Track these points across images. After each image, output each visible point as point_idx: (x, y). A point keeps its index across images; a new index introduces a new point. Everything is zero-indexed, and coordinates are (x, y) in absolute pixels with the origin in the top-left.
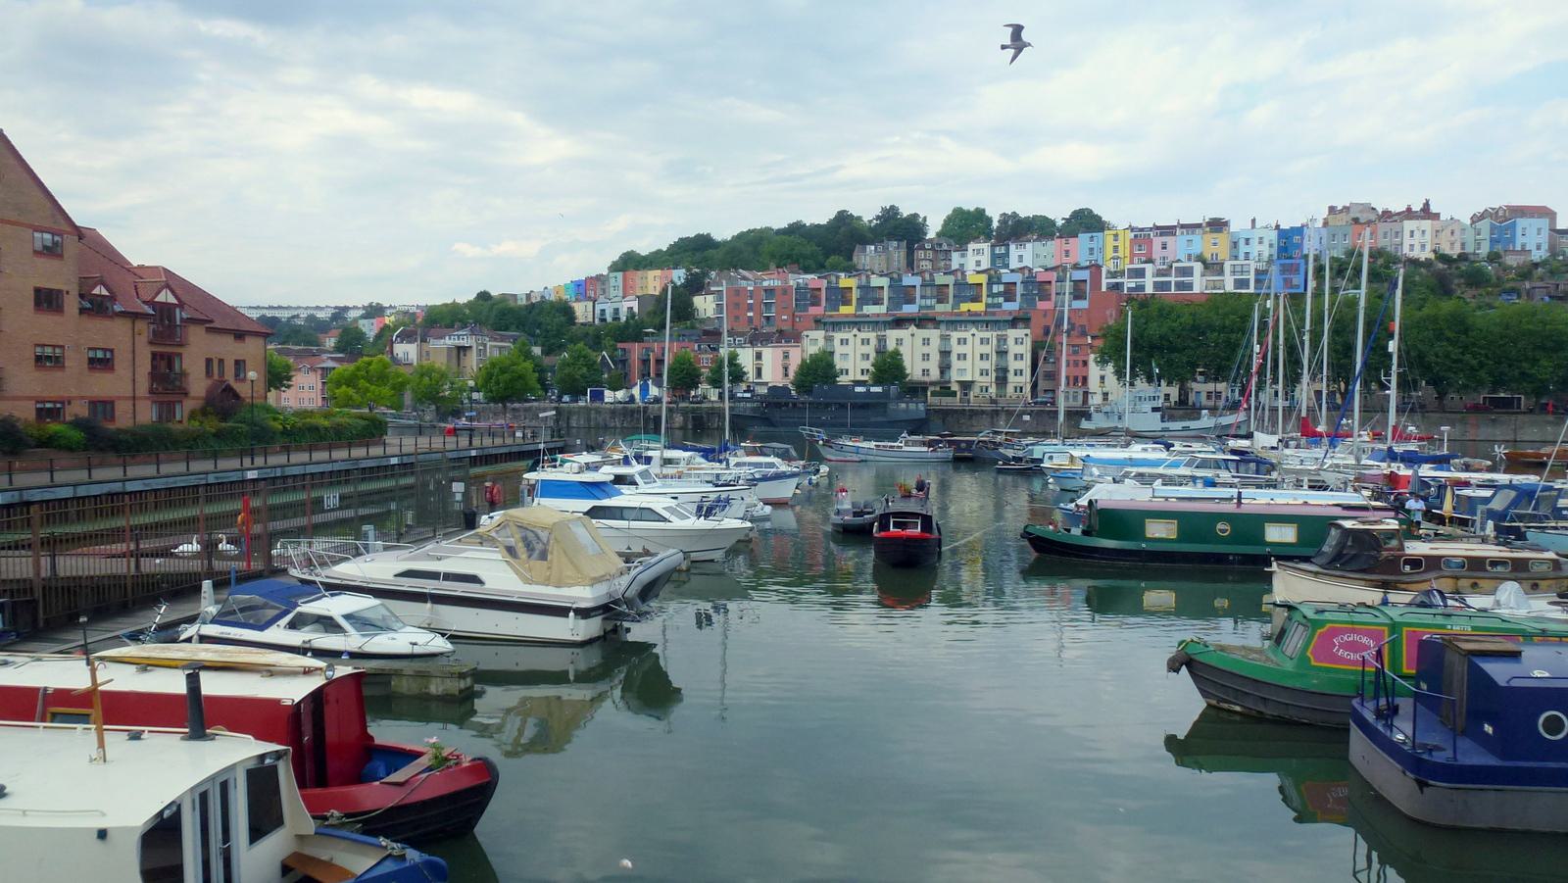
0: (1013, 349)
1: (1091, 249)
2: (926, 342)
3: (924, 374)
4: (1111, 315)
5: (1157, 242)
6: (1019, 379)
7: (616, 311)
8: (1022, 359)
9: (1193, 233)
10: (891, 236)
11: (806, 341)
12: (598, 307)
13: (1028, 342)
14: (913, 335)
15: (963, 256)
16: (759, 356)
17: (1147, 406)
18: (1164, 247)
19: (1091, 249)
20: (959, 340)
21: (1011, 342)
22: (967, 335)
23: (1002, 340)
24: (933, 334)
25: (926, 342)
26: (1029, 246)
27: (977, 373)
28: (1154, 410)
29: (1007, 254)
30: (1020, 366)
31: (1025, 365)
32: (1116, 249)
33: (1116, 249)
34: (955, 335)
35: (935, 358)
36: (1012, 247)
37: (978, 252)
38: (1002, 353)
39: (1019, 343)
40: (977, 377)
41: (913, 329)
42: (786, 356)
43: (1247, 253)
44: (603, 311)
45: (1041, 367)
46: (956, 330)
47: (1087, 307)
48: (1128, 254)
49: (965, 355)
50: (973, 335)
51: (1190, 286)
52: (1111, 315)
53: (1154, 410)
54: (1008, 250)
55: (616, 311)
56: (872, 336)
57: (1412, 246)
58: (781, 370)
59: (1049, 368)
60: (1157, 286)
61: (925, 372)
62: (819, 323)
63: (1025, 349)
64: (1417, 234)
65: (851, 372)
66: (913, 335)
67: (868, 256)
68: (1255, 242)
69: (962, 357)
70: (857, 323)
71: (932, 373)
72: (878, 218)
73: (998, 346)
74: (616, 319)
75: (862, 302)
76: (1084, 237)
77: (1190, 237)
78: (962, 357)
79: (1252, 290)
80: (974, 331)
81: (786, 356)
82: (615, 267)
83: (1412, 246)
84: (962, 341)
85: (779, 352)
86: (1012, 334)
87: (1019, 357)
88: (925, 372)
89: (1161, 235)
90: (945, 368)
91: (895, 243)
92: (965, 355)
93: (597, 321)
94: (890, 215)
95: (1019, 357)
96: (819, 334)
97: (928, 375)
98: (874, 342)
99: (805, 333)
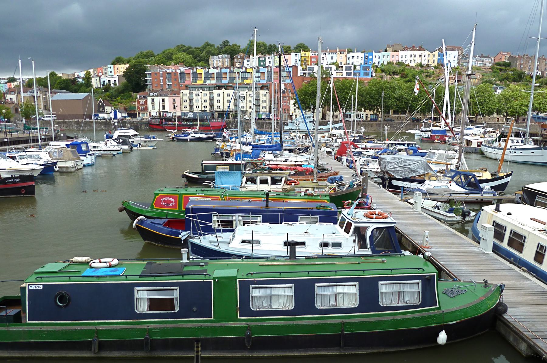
0: (262, 98)
2: (229, 95)
6: (264, 110)
10: (226, 53)
11: (181, 94)
12: (102, 80)
13: (268, 95)
15: (248, 61)
16: (163, 101)
21: (261, 95)
23: (257, 94)
24: (231, 92)
28: (310, 122)
29: (265, 61)
31: (266, 104)
36: (267, 58)
38: (257, 100)
40: (248, 109)
41: (223, 90)
42: (174, 100)
44: (104, 81)
54: (265, 59)
56: (208, 93)
58: (172, 107)
62: (187, 87)
63: (267, 98)
64: (413, 56)
65: (200, 107)
67: (215, 61)
70: (202, 87)
73: (256, 97)
75: (206, 79)
77: (332, 55)
79: (352, 76)
80: (247, 91)
81: (174, 100)
85: (171, 99)
86: (262, 92)
87: (264, 101)
88: (229, 107)
91: (226, 55)
93: (102, 86)
95: (264, 101)
96: (187, 92)
98: (208, 95)
99: (182, 91)
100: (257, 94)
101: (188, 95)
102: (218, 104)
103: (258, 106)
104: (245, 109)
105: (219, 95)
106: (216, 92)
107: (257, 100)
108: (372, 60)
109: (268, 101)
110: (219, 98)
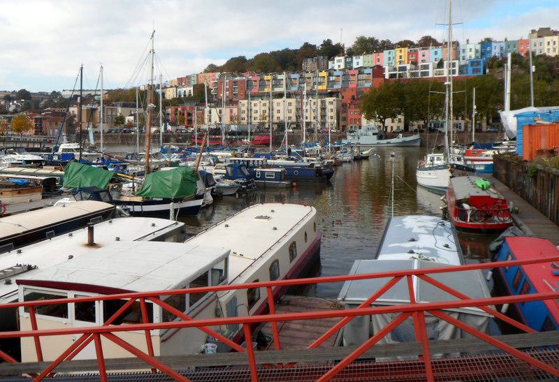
0: (329, 107)
1: (389, 58)
7: (185, 92)
17: (370, 133)
19: (389, 58)
23: (323, 102)
26: (361, 57)
27: (312, 118)
29: (352, 62)
30: (331, 114)
31: (334, 114)
32: (401, 57)
33: (401, 57)
35: (294, 110)
36: (354, 58)
37: (339, 61)
38: (323, 109)
39: (331, 104)
43: (464, 57)
48: (406, 60)
51: (426, 74)
53: (374, 134)
54: (352, 60)
55: (185, 92)
57: (549, 49)
59: (344, 115)
60: (412, 74)
61: (290, 118)
63: (333, 107)
64: (551, 43)
68: (468, 51)
72: (322, 45)
74: (185, 95)
76: (386, 52)
77: (436, 50)
82: (206, 71)
83: (549, 49)
85: (228, 110)
86: (328, 100)
89: (423, 49)
90: (298, 117)
91: (322, 57)
94: (327, 44)
100: (323, 102)
101: (246, 105)
103: (323, 116)
104: (308, 120)
105: (278, 104)
106: (276, 101)
107: (323, 109)
108: (490, 52)
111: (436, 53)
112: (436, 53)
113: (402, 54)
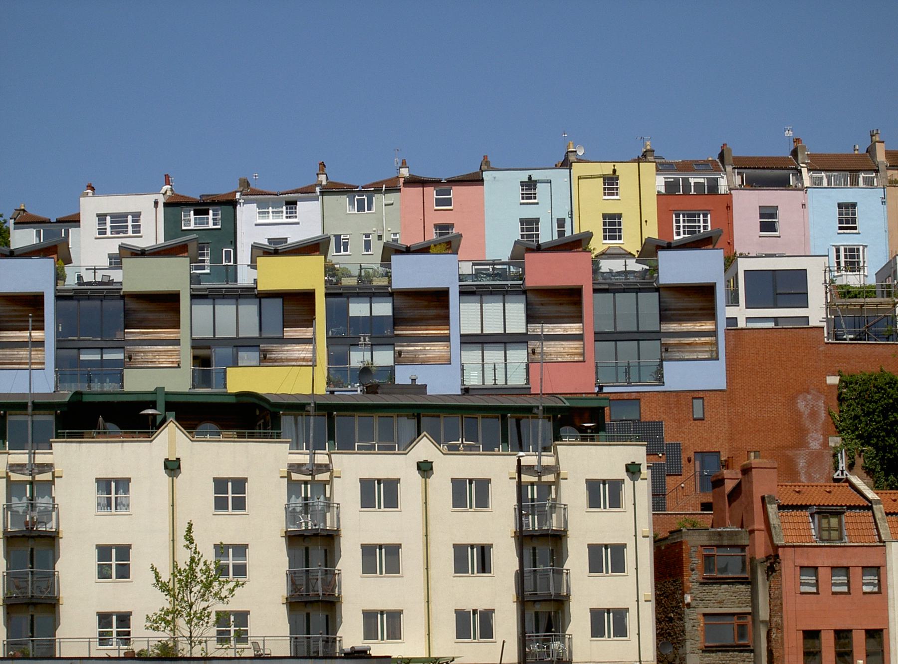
0: (585, 527)
2: (230, 493)
3: (223, 638)
4: (814, 415)
5: (747, 204)
8: (619, 566)
9: (855, 183)
14: (173, 467)
18: (768, 221)
20: (368, 488)
21: (572, 494)
22: (397, 465)
24: (264, 463)
25: (230, 493)
27: (447, 626)
34: (351, 468)
38: (541, 544)
41: (171, 438)
45: (699, 600)
46: (347, 446)
47: (720, 383)
49: (393, 551)
50: (425, 468)
52: (814, 415)
66: (173, 467)
69: (382, 558)
71: (254, 629)
77: (848, 195)
78: (382, 558)
80: (425, 448)
84: (380, 493)
86: (583, 462)
87: (607, 558)
92: (393, 551)
95: (607, 558)
97: (241, 637)
102: (115, 596)
107: (541, 544)
109: (642, 559)
110: (114, 529)
111: (847, 217)
112: (847, 217)
113: (623, 203)
